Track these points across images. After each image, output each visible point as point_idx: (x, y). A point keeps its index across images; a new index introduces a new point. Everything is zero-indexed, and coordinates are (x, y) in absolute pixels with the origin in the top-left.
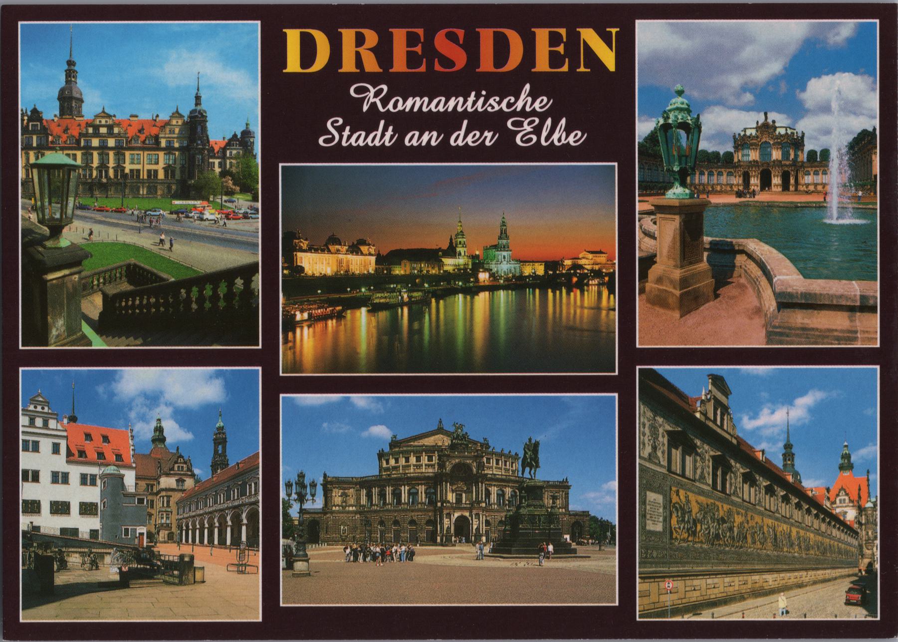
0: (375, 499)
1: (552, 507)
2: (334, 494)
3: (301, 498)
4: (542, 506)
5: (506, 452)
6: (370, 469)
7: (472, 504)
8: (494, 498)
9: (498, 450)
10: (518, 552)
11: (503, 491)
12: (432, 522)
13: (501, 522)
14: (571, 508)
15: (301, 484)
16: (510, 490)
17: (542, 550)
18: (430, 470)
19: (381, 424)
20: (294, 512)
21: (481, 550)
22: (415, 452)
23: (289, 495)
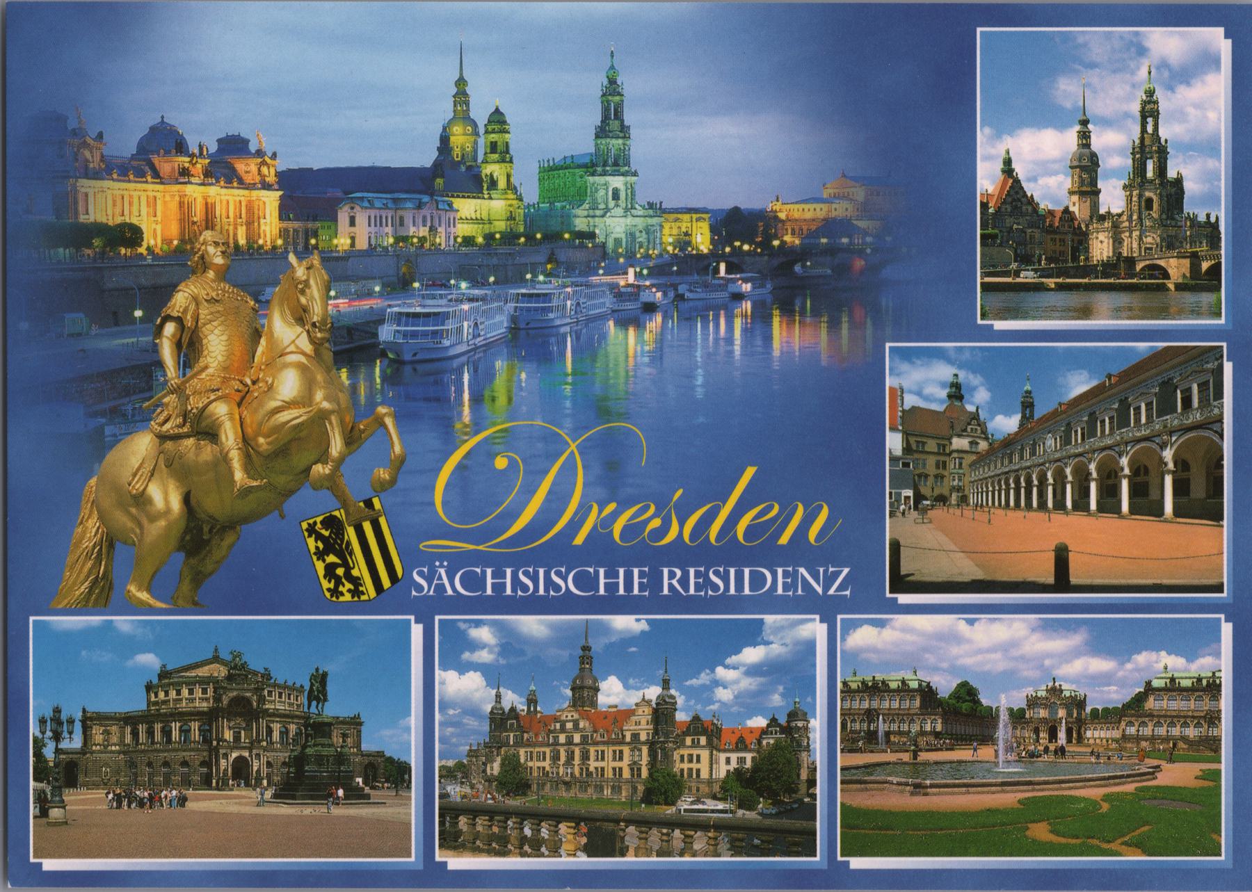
0: (142, 737)
3: (57, 737)
5: (290, 683)
6: (138, 704)
7: (251, 743)
8: (276, 736)
9: (281, 681)
13: (284, 763)
14: (364, 747)
15: (57, 720)
17: (330, 795)
18: (205, 704)
19: (149, 652)
20: (49, 752)
21: (262, 794)
22: (187, 684)
23: (43, 733)
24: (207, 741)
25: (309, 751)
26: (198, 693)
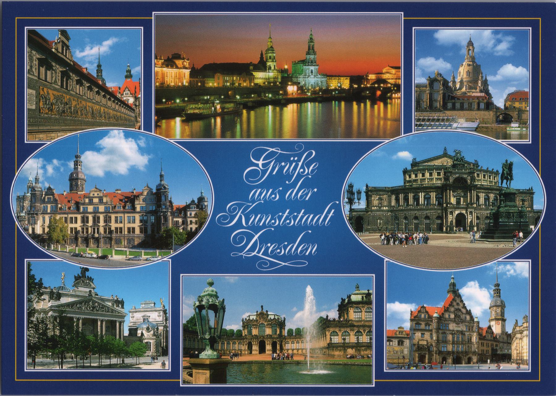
1: (522, 207)
2: (373, 199)
3: (351, 202)
4: (515, 206)
5: (490, 169)
6: (398, 181)
7: (467, 205)
8: (482, 201)
9: (485, 168)
10: (499, 238)
11: (488, 196)
12: (440, 218)
16: (493, 195)
17: (515, 236)
19: (405, 151)
21: (474, 236)
22: (429, 170)
24: (440, 204)
25: (501, 210)
26: (435, 175)
